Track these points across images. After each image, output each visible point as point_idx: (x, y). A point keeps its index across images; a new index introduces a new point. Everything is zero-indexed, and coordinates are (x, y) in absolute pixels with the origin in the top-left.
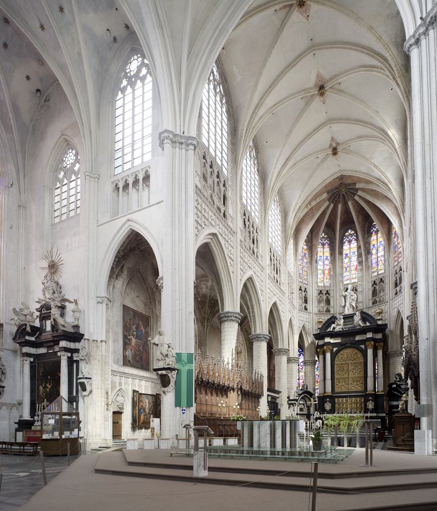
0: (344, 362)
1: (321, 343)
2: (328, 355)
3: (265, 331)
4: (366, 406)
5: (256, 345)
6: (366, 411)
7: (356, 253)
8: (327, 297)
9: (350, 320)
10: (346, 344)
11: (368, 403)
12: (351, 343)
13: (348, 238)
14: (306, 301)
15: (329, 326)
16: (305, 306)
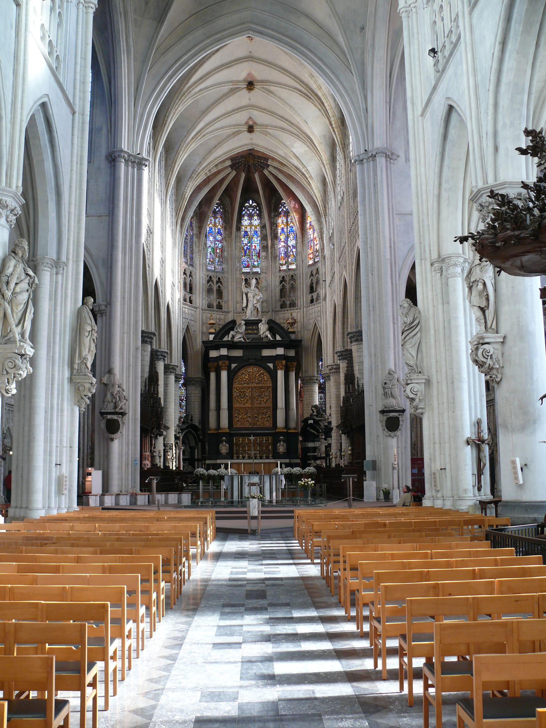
0: (245, 385)
1: (213, 354)
2: (224, 374)
4: (275, 448)
6: (276, 455)
7: (259, 233)
8: (219, 286)
9: (254, 327)
10: (249, 359)
11: (278, 445)
12: (254, 359)
13: (249, 210)
14: (191, 291)
16: (190, 297)
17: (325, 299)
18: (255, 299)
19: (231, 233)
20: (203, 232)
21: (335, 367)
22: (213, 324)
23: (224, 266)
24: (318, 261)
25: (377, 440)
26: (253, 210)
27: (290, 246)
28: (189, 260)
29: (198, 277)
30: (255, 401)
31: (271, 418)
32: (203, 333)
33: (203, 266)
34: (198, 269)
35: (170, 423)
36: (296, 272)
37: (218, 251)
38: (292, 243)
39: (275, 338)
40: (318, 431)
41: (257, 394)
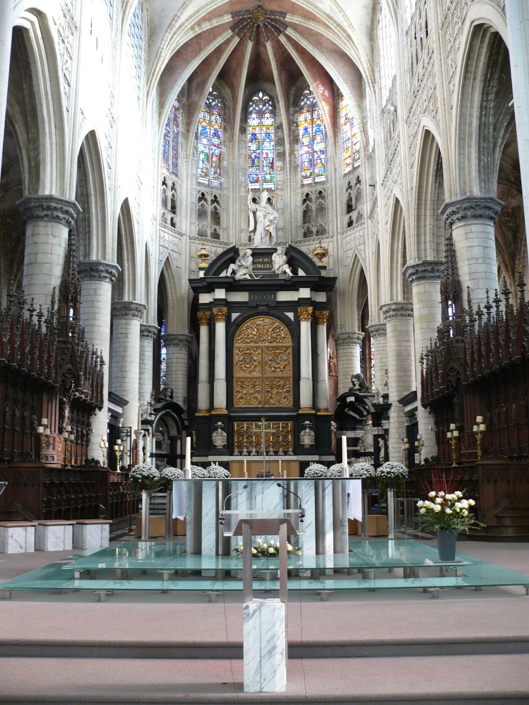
0: (252, 344)
2: (220, 328)
3: (111, 258)
5: (86, 286)
6: (299, 449)
7: (272, 136)
9: (266, 260)
10: (258, 306)
11: (302, 433)
12: (267, 306)
14: (173, 209)
15: (225, 266)
16: (172, 219)
18: (267, 220)
19: (233, 135)
20: (193, 129)
21: (393, 307)
23: (222, 180)
24: (359, 166)
26: (264, 105)
27: (316, 152)
28: (171, 167)
29: (184, 192)
30: (267, 368)
31: (291, 393)
32: (191, 271)
33: (192, 178)
34: (185, 181)
35: (131, 396)
36: (325, 186)
37: (214, 159)
40: (360, 414)
41: (270, 358)
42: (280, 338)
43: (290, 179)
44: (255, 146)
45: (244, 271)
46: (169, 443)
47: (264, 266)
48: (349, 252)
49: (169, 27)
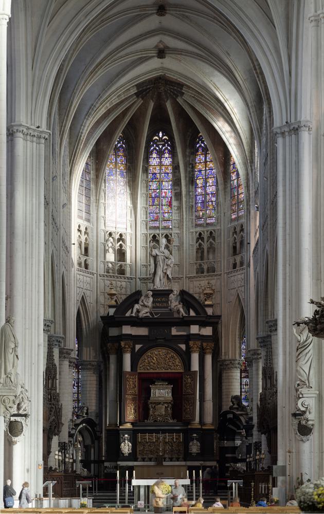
1: (113, 332)
2: (127, 358)
6: (187, 456)
7: (170, 175)
8: (121, 245)
11: (191, 444)
12: (163, 339)
13: (158, 146)
16: (86, 261)
17: (249, 265)
22: (114, 295)
25: (290, 444)
26: (164, 145)
38: (211, 189)
39: (189, 314)
42: (174, 366)
43: (186, 218)
44: (155, 186)
45: (147, 310)
46: (85, 451)
47: (161, 305)
48: (233, 290)
49: (87, 115)
